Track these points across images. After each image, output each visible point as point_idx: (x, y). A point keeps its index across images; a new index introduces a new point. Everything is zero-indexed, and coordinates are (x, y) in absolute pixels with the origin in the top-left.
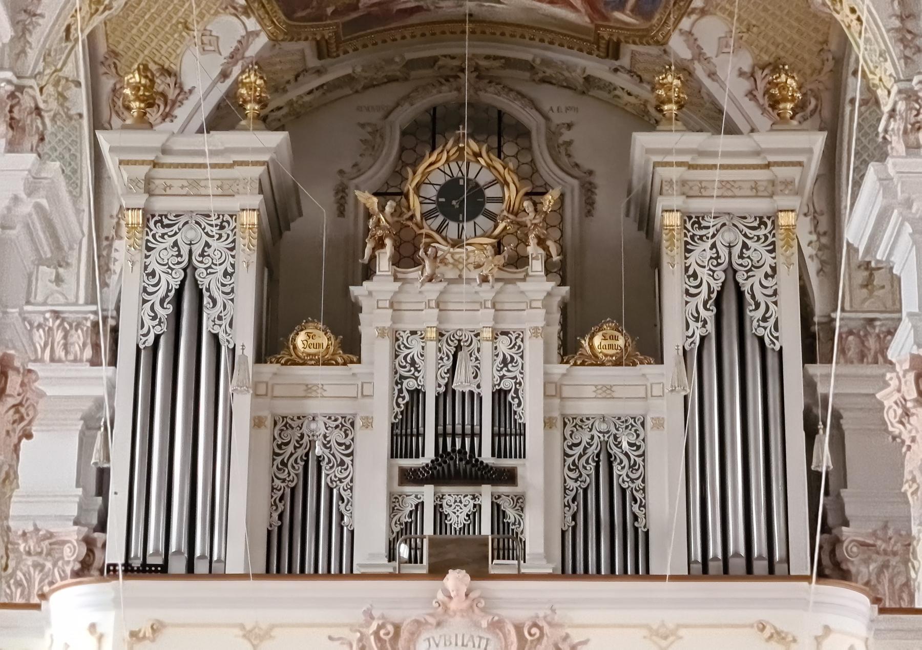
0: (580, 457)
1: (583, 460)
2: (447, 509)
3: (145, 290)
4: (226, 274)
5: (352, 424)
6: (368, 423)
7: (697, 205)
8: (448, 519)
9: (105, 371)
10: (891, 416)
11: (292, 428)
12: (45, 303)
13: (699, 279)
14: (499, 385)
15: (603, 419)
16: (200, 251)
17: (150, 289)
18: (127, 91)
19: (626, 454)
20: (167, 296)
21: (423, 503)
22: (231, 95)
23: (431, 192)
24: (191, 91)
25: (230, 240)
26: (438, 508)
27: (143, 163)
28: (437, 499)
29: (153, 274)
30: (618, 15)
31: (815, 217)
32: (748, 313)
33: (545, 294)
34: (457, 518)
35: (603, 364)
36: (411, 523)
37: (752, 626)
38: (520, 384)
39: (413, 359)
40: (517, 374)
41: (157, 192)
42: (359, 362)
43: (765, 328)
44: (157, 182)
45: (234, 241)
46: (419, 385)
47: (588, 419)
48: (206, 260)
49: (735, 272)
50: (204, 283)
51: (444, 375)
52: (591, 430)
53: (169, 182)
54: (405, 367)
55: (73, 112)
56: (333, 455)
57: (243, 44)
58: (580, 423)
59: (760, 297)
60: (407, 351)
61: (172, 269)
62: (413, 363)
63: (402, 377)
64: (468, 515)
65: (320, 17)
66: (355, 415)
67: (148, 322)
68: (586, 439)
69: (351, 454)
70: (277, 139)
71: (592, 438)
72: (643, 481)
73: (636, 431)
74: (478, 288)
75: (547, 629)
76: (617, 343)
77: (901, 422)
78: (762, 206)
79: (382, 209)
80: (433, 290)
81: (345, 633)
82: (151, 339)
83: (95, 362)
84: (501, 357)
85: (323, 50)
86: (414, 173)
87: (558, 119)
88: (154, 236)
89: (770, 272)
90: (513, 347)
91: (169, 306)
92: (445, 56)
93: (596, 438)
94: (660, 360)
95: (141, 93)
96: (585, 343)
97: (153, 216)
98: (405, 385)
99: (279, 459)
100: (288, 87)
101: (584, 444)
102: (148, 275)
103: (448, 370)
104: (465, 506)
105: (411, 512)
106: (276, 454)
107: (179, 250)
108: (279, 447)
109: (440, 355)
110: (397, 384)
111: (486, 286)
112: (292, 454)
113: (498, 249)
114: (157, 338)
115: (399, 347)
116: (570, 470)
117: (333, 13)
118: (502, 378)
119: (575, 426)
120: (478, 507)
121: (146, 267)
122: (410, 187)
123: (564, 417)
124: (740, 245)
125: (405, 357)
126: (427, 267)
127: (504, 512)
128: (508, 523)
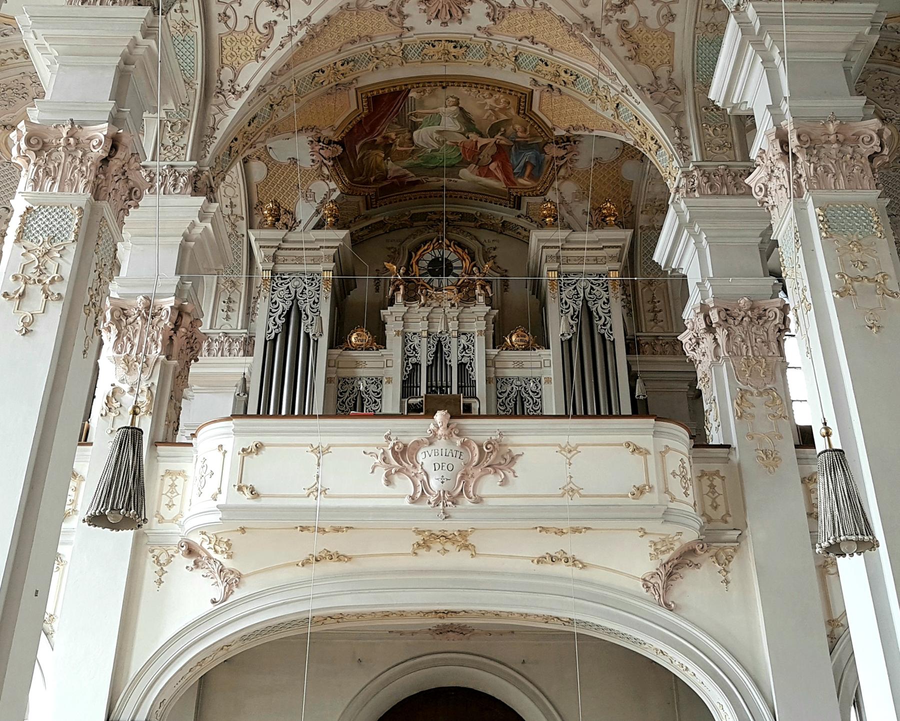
0: (506, 398)
1: (509, 399)
3: (271, 310)
4: (314, 303)
5: (381, 382)
6: (389, 381)
9: (249, 359)
10: (687, 348)
11: (348, 384)
12: (220, 329)
13: (568, 305)
14: (461, 360)
15: (518, 379)
16: (301, 291)
17: (274, 310)
18: (266, 212)
19: (531, 397)
20: (282, 314)
23: (424, 264)
24: (300, 222)
25: (317, 286)
27: (272, 247)
29: (275, 303)
30: (521, 181)
31: (623, 288)
32: (595, 321)
33: (485, 313)
35: (517, 350)
38: (473, 360)
39: (414, 347)
40: (471, 354)
41: (279, 262)
42: (385, 348)
43: (605, 329)
44: (279, 258)
45: (319, 287)
47: (510, 379)
48: (304, 296)
49: (587, 301)
50: (302, 306)
51: (431, 355)
52: (512, 384)
53: (286, 258)
54: (410, 351)
55: (239, 234)
56: (370, 398)
58: (505, 381)
59: (601, 314)
60: (412, 343)
61: (286, 300)
62: (414, 349)
63: (408, 357)
65: (368, 183)
66: (382, 377)
67: (272, 327)
68: (509, 389)
69: (380, 397)
70: (343, 233)
71: (512, 388)
72: (541, 411)
73: (536, 385)
74: (450, 310)
76: (525, 339)
77: (694, 350)
82: (273, 335)
84: (462, 346)
86: (416, 255)
87: (487, 245)
88: (277, 284)
89: (606, 301)
90: (469, 341)
91: (284, 319)
92: (431, 212)
93: (514, 389)
94: (549, 348)
95: (273, 212)
97: (277, 274)
98: (410, 361)
99: (341, 400)
100: (351, 225)
101: (508, 391)
102: (273, 303)
103: (434, 353)
106: (338, 397)
107: (290, 291)
108: (341, 394)
109: (429, 345)
110: (406, 360)
111: (453, 309)
112: (348, 398)
113: (459, 291)
114: (276, 335)
115: (407, 341)
116: (500, 405)
117: (375, 180)
118: (463, 357)
119: (503, 383)
121: (272, 299)
122: (413, 261)
123: (496, 377)
124: (589, 288)
125: (410, 347)
126: (422, 300)
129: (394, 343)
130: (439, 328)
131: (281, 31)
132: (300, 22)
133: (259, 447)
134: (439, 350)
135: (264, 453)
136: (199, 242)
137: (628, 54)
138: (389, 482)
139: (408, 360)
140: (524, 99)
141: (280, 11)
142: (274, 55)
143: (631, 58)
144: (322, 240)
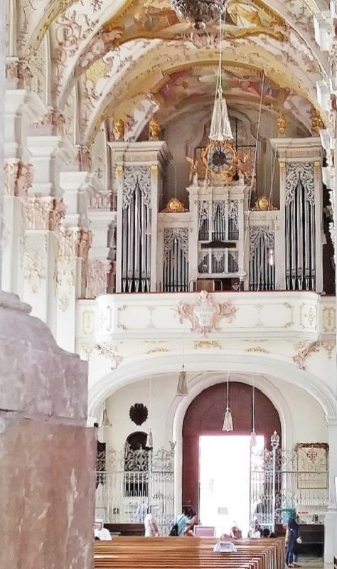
6: (192, 231)
7: (290, 160)
22: (147, 127)
24: (137, 122)
26: (213, 256)
34: (218, 258)
37: (283, 304)
49: (301, 181)
57: (151, 109)
59: (309, 189)
62: (205, 211)
70: (161, 143)
75: (228, 307)
78: (310, 160)
79: (195, 163)
80: (210, 189)
81: (175, 307)
83: (111, 209)
85: (177, 107)
94: (279, 209)
96: (257, 204)
129: (193, 207)
130: (217, 198)
131: (116, 63)
132: (126, 59)
133: (125, 307)
134: (218, 209)
135: (128, 308)
136: (87, 190)
137: (309, 69)
138: (181, 321)
140: (261, 73)
141: (115, 52)
142: (115, 77)
143: (310, 71)
144: (151, 147)
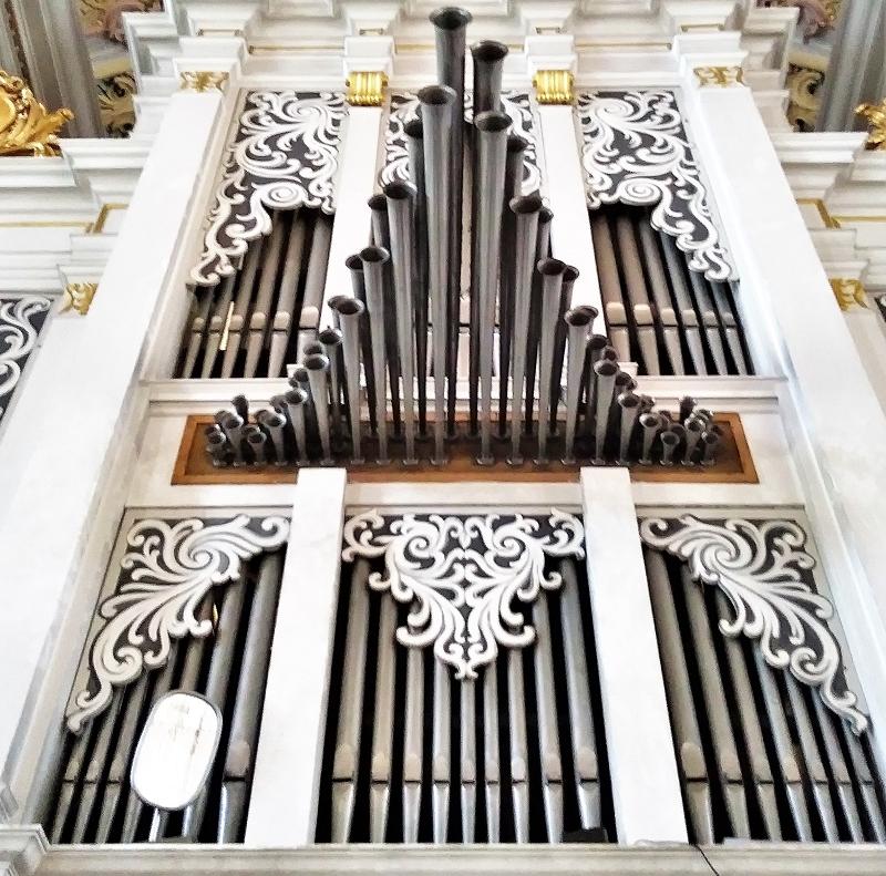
2: (402, 580)
8: (415, 619)
14: (611, 191)
21: (281, 551)
28: (357, 533)
36: (210, 641)
38: (691, 189)
46: (311, 197)
60: (278, 128)
63: (249, 179)
64: (516, 605)
84: (611, 137)
104: (503, 562)
105: (217, 593)
109: (393, 137)
118: (617, 178)
120: (567, 568)
127: (711, 592)
128: (747, 644)
139: (248, 195)
